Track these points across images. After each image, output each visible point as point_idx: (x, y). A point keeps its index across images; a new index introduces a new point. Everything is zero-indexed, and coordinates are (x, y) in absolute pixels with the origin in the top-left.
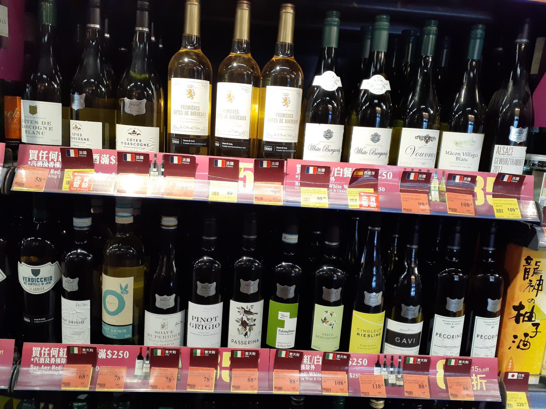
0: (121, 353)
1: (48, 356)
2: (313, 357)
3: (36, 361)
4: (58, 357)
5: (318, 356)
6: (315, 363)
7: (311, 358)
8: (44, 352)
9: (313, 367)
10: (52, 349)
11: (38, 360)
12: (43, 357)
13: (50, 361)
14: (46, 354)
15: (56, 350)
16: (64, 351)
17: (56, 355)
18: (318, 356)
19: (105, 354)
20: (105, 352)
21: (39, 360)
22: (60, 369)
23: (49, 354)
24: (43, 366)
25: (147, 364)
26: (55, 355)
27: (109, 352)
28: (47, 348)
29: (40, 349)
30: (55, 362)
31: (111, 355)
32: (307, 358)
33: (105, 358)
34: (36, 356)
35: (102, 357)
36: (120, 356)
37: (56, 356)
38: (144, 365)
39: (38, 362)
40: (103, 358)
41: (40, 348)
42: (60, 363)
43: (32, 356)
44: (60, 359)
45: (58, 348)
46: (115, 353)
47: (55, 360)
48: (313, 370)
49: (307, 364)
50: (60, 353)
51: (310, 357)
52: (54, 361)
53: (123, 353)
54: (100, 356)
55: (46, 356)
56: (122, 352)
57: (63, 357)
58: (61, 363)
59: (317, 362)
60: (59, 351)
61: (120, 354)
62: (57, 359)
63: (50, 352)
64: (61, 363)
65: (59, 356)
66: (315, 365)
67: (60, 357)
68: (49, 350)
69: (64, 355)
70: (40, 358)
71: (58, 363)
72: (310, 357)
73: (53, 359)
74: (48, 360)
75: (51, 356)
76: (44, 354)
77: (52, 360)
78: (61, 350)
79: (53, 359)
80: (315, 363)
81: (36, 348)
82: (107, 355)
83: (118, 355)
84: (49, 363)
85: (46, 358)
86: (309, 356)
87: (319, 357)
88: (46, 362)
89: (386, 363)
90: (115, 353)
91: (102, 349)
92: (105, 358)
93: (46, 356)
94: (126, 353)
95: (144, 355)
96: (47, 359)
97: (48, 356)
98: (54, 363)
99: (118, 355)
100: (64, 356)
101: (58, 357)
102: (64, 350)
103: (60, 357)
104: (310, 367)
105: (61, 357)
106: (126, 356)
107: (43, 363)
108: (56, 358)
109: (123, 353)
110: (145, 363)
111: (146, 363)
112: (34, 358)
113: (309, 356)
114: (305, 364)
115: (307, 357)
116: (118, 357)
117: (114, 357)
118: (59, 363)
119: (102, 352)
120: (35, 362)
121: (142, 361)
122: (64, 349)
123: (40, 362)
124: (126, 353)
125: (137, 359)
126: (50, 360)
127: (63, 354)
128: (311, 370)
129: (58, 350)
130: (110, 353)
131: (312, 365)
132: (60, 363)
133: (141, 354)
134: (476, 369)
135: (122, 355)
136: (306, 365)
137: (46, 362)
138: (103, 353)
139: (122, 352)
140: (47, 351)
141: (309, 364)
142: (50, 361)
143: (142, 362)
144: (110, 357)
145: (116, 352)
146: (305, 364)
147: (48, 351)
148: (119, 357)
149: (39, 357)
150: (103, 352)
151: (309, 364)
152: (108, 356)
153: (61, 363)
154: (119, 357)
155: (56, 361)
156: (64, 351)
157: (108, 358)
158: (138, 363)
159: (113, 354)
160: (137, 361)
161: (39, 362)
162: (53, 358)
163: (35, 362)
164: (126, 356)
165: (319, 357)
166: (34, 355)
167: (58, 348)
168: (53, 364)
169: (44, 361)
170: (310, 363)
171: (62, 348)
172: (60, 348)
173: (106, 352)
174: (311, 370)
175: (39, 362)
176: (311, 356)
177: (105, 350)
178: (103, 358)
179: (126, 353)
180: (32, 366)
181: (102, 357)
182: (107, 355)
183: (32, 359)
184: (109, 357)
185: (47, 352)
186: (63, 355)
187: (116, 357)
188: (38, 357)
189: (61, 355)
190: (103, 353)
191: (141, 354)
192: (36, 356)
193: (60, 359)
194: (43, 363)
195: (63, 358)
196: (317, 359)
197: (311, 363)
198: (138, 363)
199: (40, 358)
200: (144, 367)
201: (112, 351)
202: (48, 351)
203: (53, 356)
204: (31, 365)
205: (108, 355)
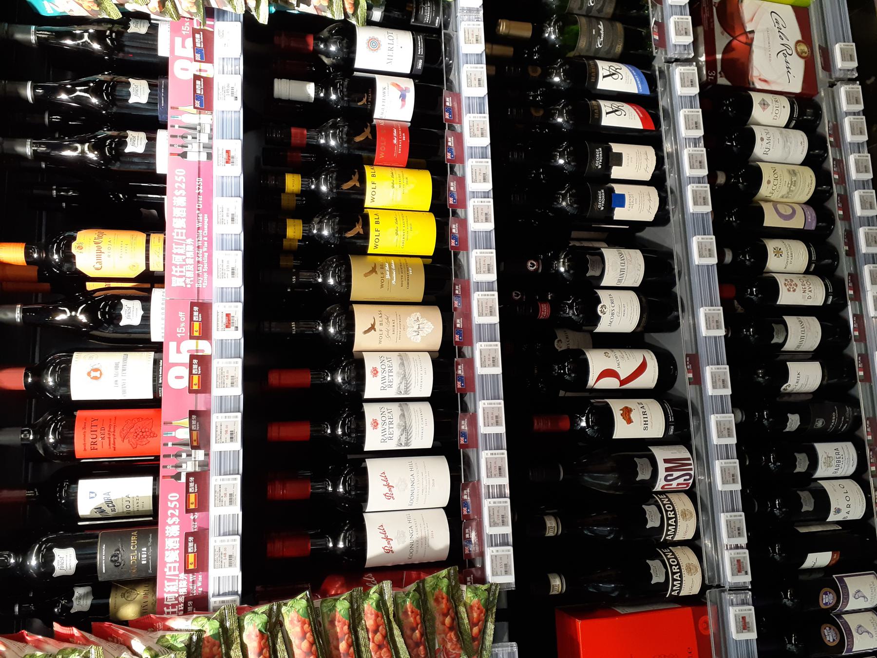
1: (177, 607)
5: (173, 234)
6: (184, 237)
7: (177, 244)
9: (189, 241)
27: (170, 521)
32: (177, 248)
33: (179, 526)
36: (176, 505)
53: (172, 502)
61: (173, 506)
78: (167, 591)
80: (184, 237)
82: (174, 524)
83: (174, 508)
89: (181, 144)
92: (179, 526)
93: (176, 610)
103: (178, 590)
109: (172, 502)
113: (174, 246)
131: (187, 243)
133: (172, 477)
134: (187, 28)
135: (174, 503)
139: (169, 503)
140: (168, 610)
148: (178, 506)
152: (176, 523)
154: (178, 506)
155: (183, 594)
159: (173, 515)
172: (165, 592)
173: (170, 525)
176: (174, 244)
182: (174, 524)
191: (172, 477)
203: (176, 600)
205: (175, 522)
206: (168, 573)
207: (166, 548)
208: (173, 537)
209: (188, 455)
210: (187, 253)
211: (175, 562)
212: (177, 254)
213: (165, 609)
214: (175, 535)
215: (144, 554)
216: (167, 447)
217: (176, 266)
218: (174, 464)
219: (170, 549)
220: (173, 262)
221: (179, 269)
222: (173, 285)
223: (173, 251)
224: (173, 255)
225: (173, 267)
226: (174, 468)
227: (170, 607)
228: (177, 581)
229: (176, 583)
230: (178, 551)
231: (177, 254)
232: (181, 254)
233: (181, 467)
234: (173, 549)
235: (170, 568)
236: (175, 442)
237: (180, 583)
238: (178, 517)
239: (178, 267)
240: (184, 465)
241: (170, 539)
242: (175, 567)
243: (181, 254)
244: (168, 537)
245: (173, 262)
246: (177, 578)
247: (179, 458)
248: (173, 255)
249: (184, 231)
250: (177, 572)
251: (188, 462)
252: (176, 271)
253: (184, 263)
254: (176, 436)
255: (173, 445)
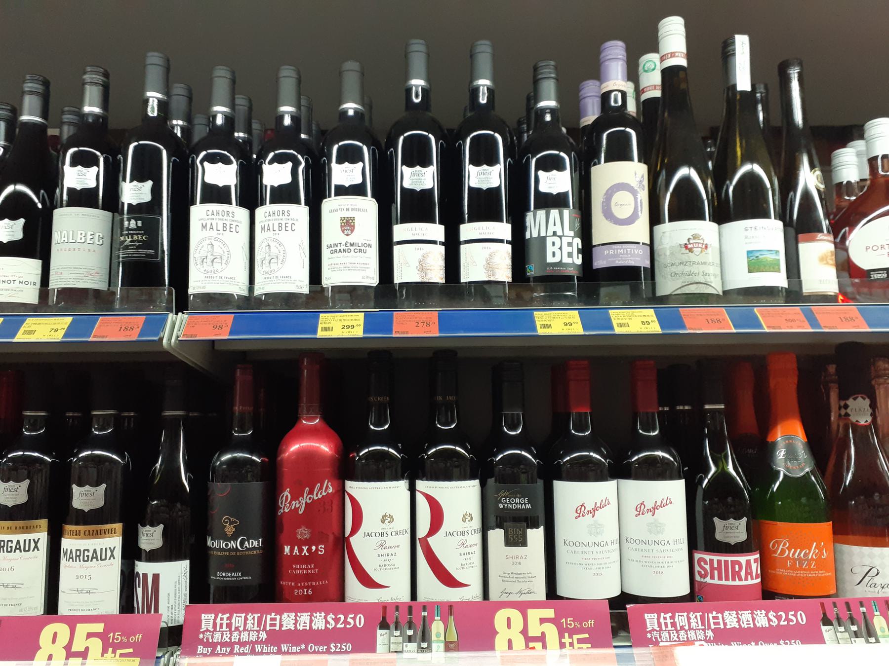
0: (350, 618)
1: (228, 629)
2: (706, 614)
3: (207, 639)
4: (245, 630)
6: (713, 627)
8: (222, 622)
10: (235, 615)
11: (210, 637)
12: (219, 631)
13: (230, 638)
14: (224, 626)
15: (241, 617)
16: (254, 619)
17: (240, 627)
18: (714, 613)
19: (324, 620)
20: (323, 617)
21: (212, 637)
22: (247, 652)
23: (229, 625)
24: (219, 647)
25: (396, 636)
26: (240, 626)
27: (330, 617)
28: (226, 614)
29: (213, 618)
30: (239, 639)
31: (332, 622)
32: (696, 617)
33: (323, 628)
34: (207, 630)
35: (318, 628)
36: (350, 624)
37: (241, 629)
38: (392, 638)
39: (211, 641)
40: (320, 629)
41: (213, 615)
42: (247, 641)
43: (201, 630)
44: (248, 632)
45: (244, 615)
46: (340, 618)
47: (240, 635)
48: (712, 639)
49: (699, 629)
50: (248, 622)
51: (700, 615)
52: (238, 637)
53: (354, 619)
54: (315, 625)
55: (224, 629)
56: (352, 616)
57: (252, 629)
58: (249, 640)
59: (715, 624)
60: (246, 619)
62: (242, 634)
63: (230, 621)
64: (250, 641)
65: (247, 628)
66: (712, 630)
67: (247, 630)
68: (229, 618)
69: (254, 626)
70: (215, 633)
71: (244, 640)
72: (700, 615)
73: (236, 634)
74: (227, 637)
75: (233, 629)
76: (221, 625)
77: (234, 635)
78: (248, 617)
79: (236, 634)
81: (206, 615)
82: (327, 622)
83: (346, 622)
84: (229, 641)
85: (225, 633)
86: (698, 615)
87: (716, 614)
88: (225, 639)
90: (340, 618)
91: (318, 613)
93: (224, 629)
94: (360, 618)
95: (391, 621)
96: (226, 634)
97: (228, 629)
98: (237, 641)
99: (346, 622)
100: (253, 628)
101: (245, 630)
102: (254, 617)
103: (247, 630)
104: (705, 633)
105: (249, 629)
106: (360, 625)
107: (220, 641)
108: (240, 632)
109: (354, 619)
110: (393, 636)
111: (395, 635)
112: (203, 633)
114: (695, 630)
115: (694, 616)
116: (345, 626)
117: (339, 626)
118: (246, 641)
119: (318, 617)
120: (205, 641)
121: (387, 631)
122: (254, 615)
123: (214, 641)
124: (360, 618)
125: (378, 628)
126: (231, 635)
127: (253, 624)
128: (708, 639)
129: (245, 616)
130: (332, 619)
131: (707, 630)
132: (247, 641)
133: (384, 618)
135: (352, 621)
136: (697, 631)
137: (225, 639)
138: (320, 620)
139: (352, 616)
141: (702, 630)
142: (230, 638)
143: (387, 635)
144: (333, 627)
145: (342, 617)
146: (695, 630)
147: (227, 620)
148: (348, 626)
149: (213, 632)
150: (320, 618)
151: (702, 630)
152: (328, 626)
153: (249, 640)
154: (348, 626)
155: (241, 638)
156: (254, 619)
157: (329, 628)
158: (382, 636)
159: (337, 620)
160: (380, 632)
161: (212, 641)
162: (236, 633)
163: (205, 641)
164: (360, 625)
165: (716, 614)
166: (204, 628)
167: (244, 615)
168: (235, 643)
169: (220, 637)
170: (703, 627)
171: (250, 614)
172: (247, 614)
173: (325, 618)
174: (708, 639)
175: (212, 641)
176: (701, 613)
177: (323, 613)
178: (320, 629)
179: (360, 617)
180: (201, 648)
181: (318, 628)
182: (327, 622)
183: (201, 636)
184: (331, 627)
185: (225, 622)
186: (252, 626)
187: (342, 626)
188: (210, 631)
189: (249, 626)
190: (320, 620)
191: (384, 618)
192: (207, 630)
193: (248, 632)
194: (220, 641)
195: (253, 631)
196: (714, 618)
197: (705, 626)
198: (381, 635)
199: (215, 633)
200: (391, 642)
201: (336, 617)
202: (227, 620)
204: (199, 647)
206: (269, 617)
207: (299, 614)
208: (311, 621)
209: (410, 637)
210: (693, 632)
211: (281, 626)
212: (689, 619)
213: (228, 615)
214: (313, 624)
215: (302, 566)
216: (422, 610)
217: (672, 617)
218: (400, 620)
219: (298, 618)
220: (677, 614)
221: (669, 621)
222: (646, 615)
223: (692, 613)
224: (685, 614)
225: (670, 614)
226: (395, 620)
227: (229, 621)
228: (258, 629)
229: (256, 628)
230: (293, 629)
231: (689, 619)
232: (689, 624)
233: (396, 629)
234: (296, 621)
235: (275, 619)
236: (427, 620)
237: (255, 632)
238: (335, 628)
239: (672, 621)
240: (398, 633)
241: (309, 617)
242: (275, 625)
243: (689, 624)
244: (311, 616)
245: (677, 614)
246: (262, 629)
247: (407, 626)
248: (685, 614)
249: (722, 626)
250: (268, 628)
251: (401, 638)
252: (665, 618)
253: (679, 628)
254: (435, 622)
255: (424, 617)
